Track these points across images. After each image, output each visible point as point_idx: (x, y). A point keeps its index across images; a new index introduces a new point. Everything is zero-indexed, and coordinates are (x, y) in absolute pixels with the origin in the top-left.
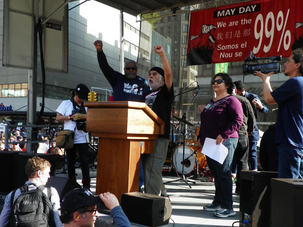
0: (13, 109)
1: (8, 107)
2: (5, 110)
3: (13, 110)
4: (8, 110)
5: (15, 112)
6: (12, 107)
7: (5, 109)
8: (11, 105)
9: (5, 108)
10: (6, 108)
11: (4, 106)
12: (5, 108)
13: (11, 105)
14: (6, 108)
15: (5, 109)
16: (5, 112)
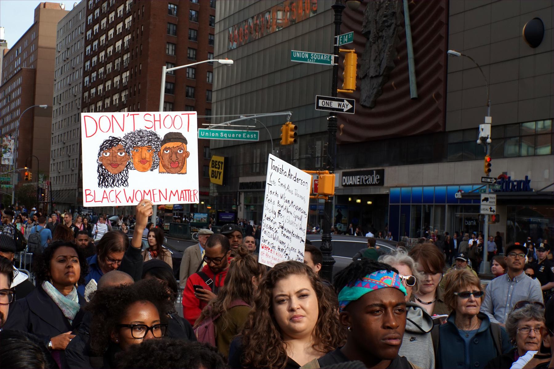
0: (531, 185)
1: (519, 182)
2: (512, 191)
3: (532, 189)
4: (520, 190)
5: (539, 193)
6: (529, 181)
7: (513, 186)
8: (527, 177)
9: (513, 184)
10: (515, 183)
11: (509, 178)
12: (513, 184)
13: (527, 177)
14: (515, 183)
15: (513, 186)
16: (512, 193)
